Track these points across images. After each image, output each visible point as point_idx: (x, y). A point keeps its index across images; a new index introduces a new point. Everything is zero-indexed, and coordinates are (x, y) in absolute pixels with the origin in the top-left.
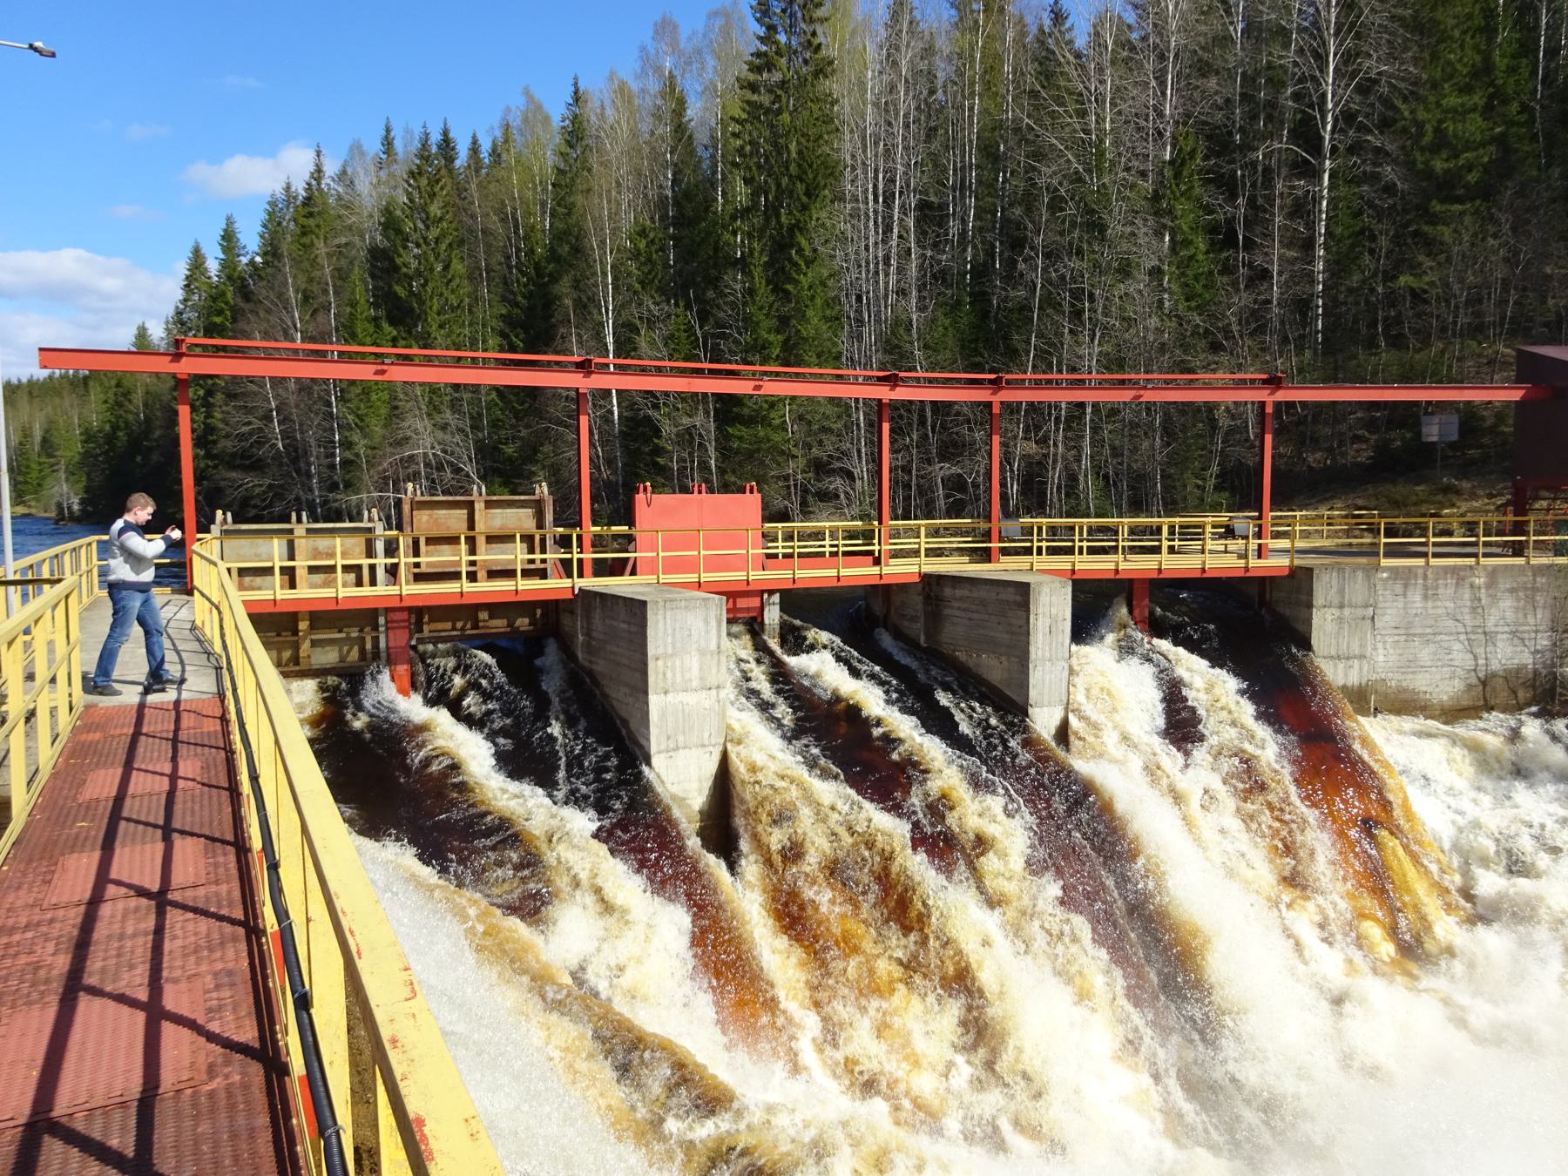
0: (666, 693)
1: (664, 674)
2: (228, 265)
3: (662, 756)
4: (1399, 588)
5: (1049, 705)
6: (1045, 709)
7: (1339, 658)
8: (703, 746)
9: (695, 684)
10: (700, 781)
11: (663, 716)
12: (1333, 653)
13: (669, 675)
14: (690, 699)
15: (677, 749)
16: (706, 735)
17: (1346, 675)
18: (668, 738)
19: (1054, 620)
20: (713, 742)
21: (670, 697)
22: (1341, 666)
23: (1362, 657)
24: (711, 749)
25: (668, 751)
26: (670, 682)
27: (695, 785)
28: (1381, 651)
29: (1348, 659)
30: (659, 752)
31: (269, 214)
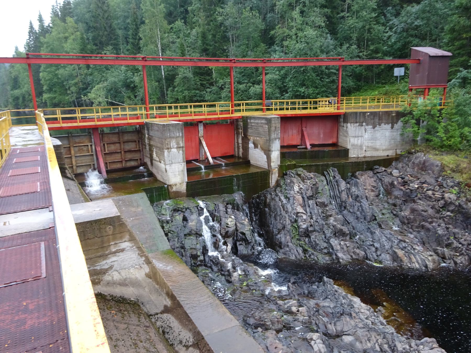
2: (42, 26)
4: (372, 117)
7: (355, 137)
8: (179, 163)
10: (179, 172)
12: (354, 135)
15: (172, 163)
17: (357, 142)
19: (276, 127)
22: (356, 139)
23: (362, 136)
27: (177, 173)
28: (367, 135)
29: (358, 137)
31: (52, 9)
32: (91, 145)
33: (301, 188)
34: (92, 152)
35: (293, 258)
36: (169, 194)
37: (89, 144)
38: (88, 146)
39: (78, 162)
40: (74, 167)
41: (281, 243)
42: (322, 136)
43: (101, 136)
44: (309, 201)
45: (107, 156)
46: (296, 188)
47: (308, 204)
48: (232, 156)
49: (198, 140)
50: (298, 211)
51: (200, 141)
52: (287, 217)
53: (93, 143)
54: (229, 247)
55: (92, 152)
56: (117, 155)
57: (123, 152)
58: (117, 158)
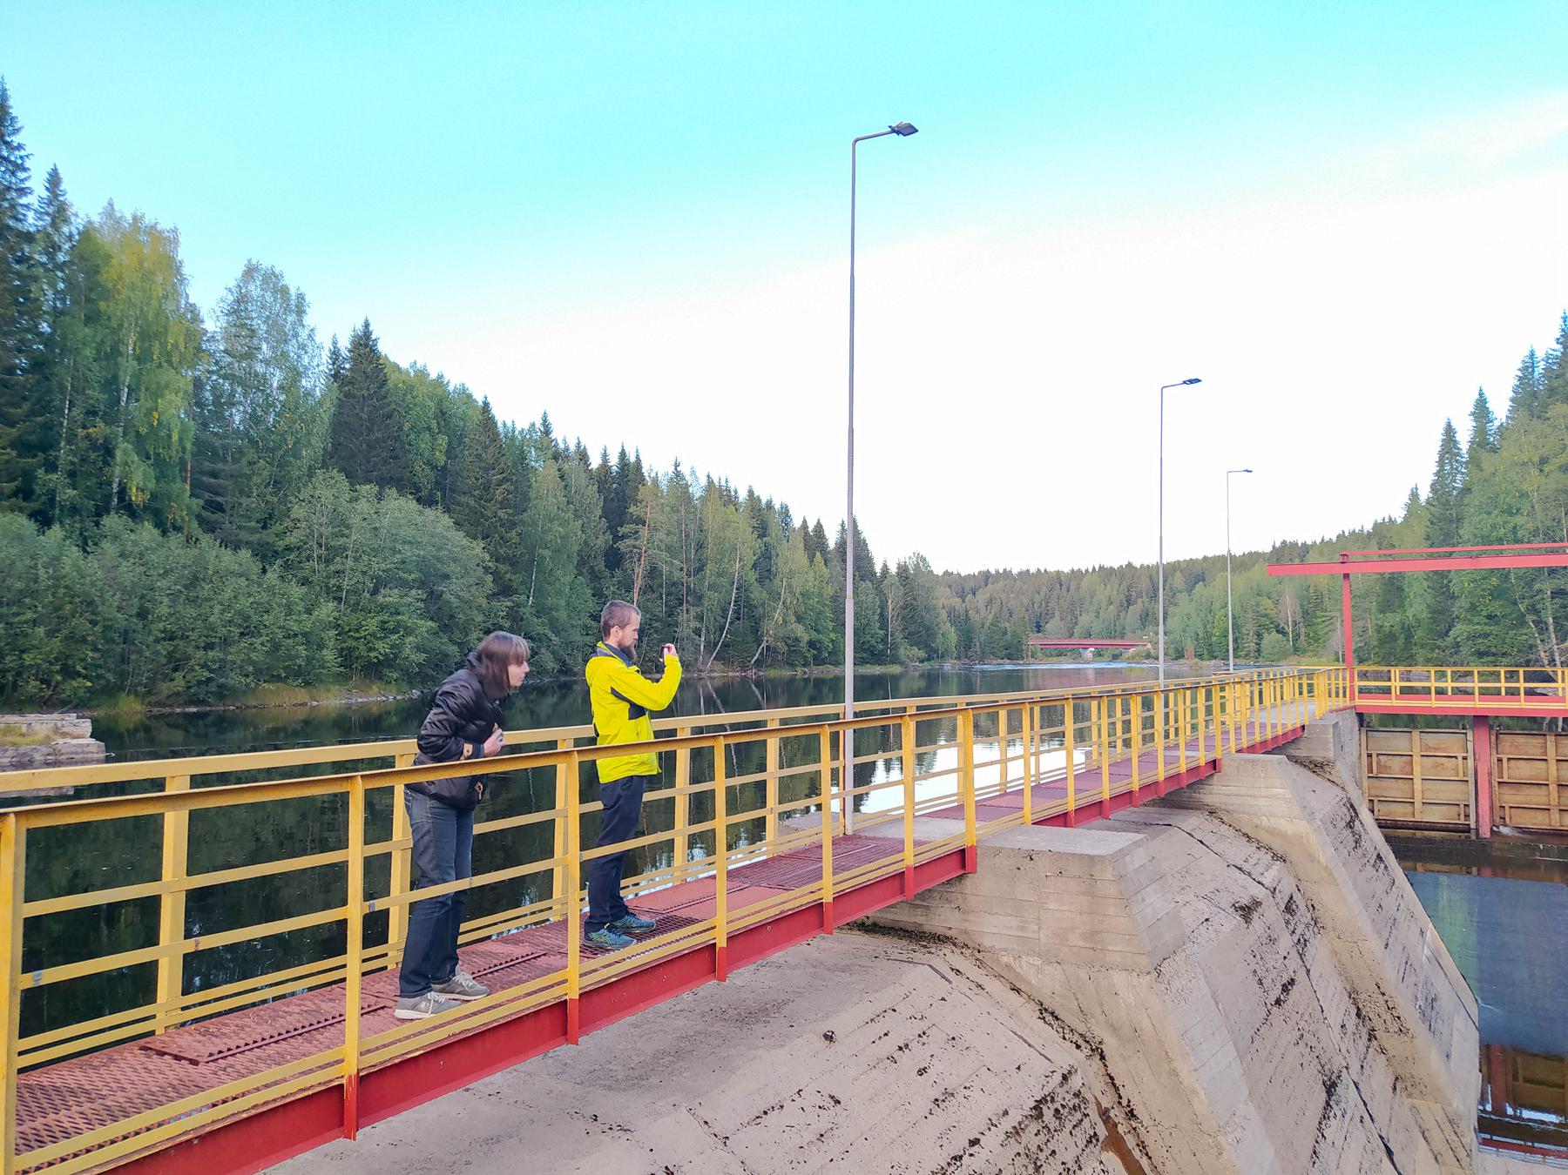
32: (1465, 758)
34: (1465, 774)
37: (1460, 755)
38: (1456, 757)
39: (1428, 795)
40: (1418, 805)
43: (1493, 738)
45: (1505, 789)
53: (1470, 755)
55: (1465, 774)
56: (1535, 790)
57: (1553, 787)
58: (1535, 799)
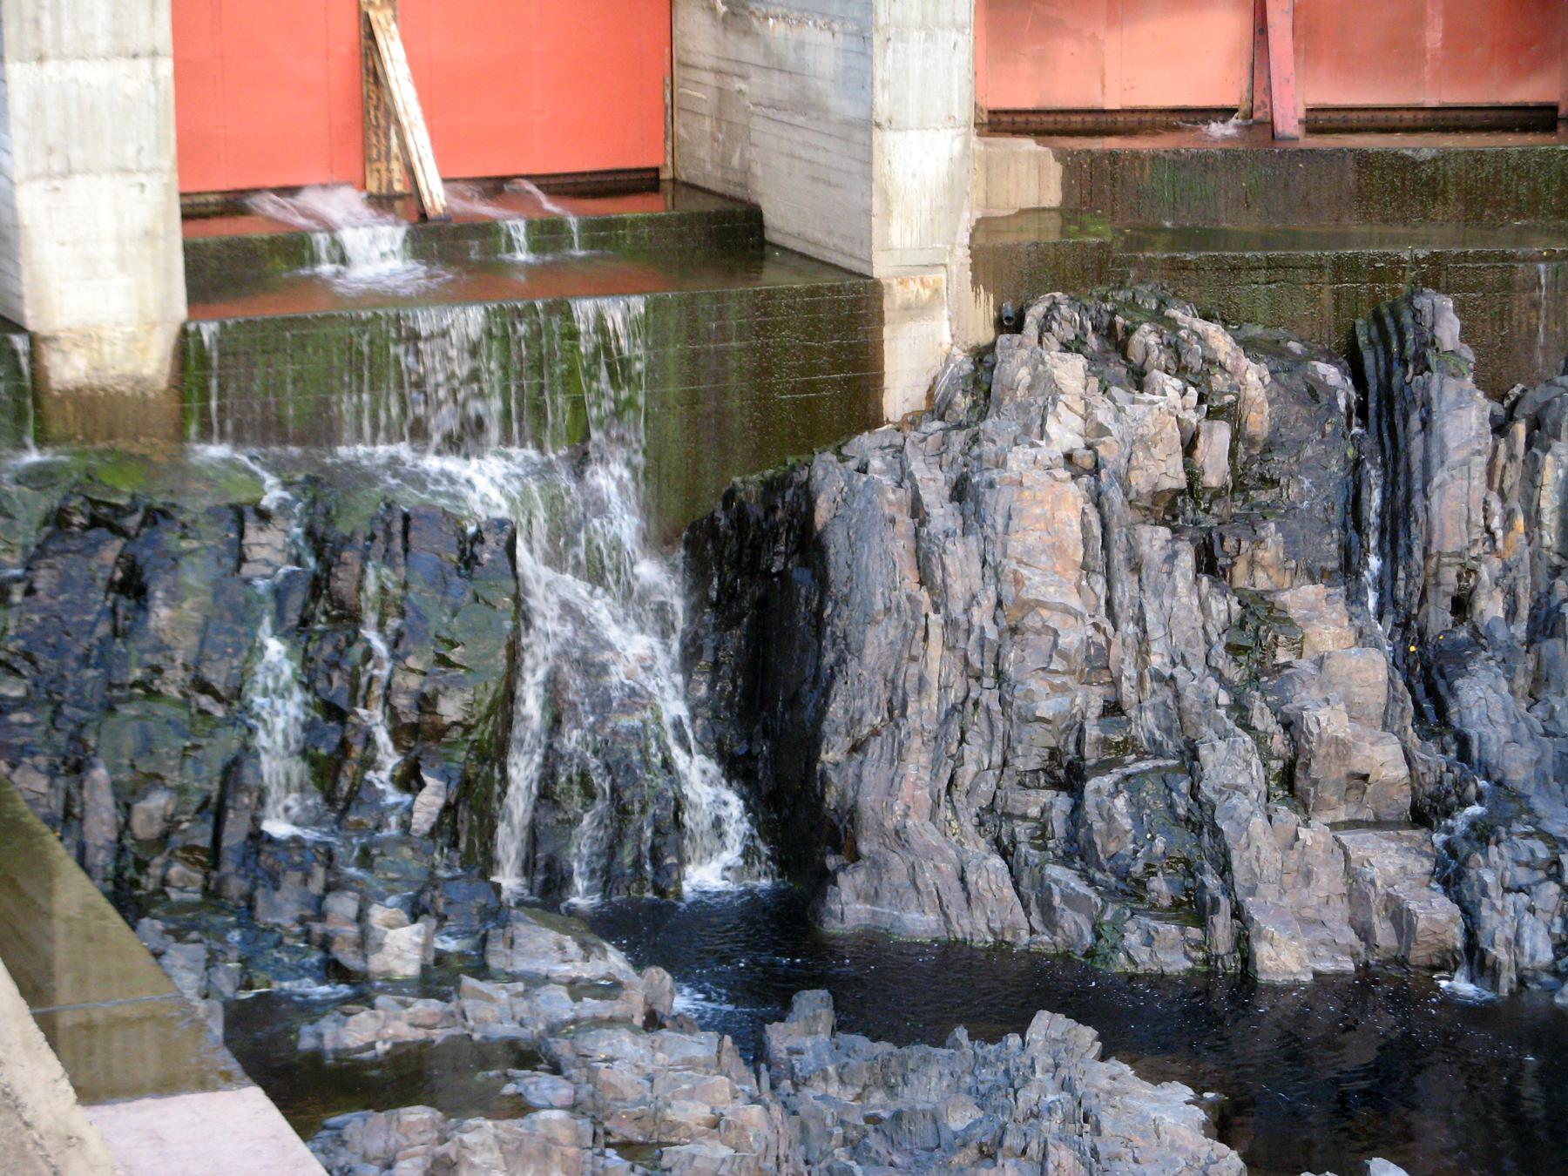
0: (41, 59)
1: (37, 22)
3: (40, 185)
5: (922, 127)
6: (913, 135)
8: (125, 170)
9: (102, 44)
10: (120, 240)
11: (37, 107)
13: (47, 22)
14: (94, 74)
15: (68, 173)
16: (131, 150)
18: (50, 151)
20: (146, 164)
21: (51, 67)
24: (142, 178)
25: (49, 175)
26: (48, 37)
30: (32, 177)
33: (1102, 430)
35: (920, 923)
36: (37, 403)
41: (852, 814)
42: (1434, 37)
44: (1145, 532)
46: (1065, 432)
47: (1132, 548)
48: (644, 182)
49: (348, 31)
50: (1031, 595)
51: (371, 36)
52: (936, 632)
54: (430, 801)
